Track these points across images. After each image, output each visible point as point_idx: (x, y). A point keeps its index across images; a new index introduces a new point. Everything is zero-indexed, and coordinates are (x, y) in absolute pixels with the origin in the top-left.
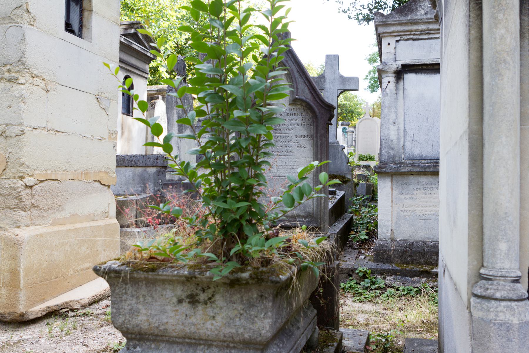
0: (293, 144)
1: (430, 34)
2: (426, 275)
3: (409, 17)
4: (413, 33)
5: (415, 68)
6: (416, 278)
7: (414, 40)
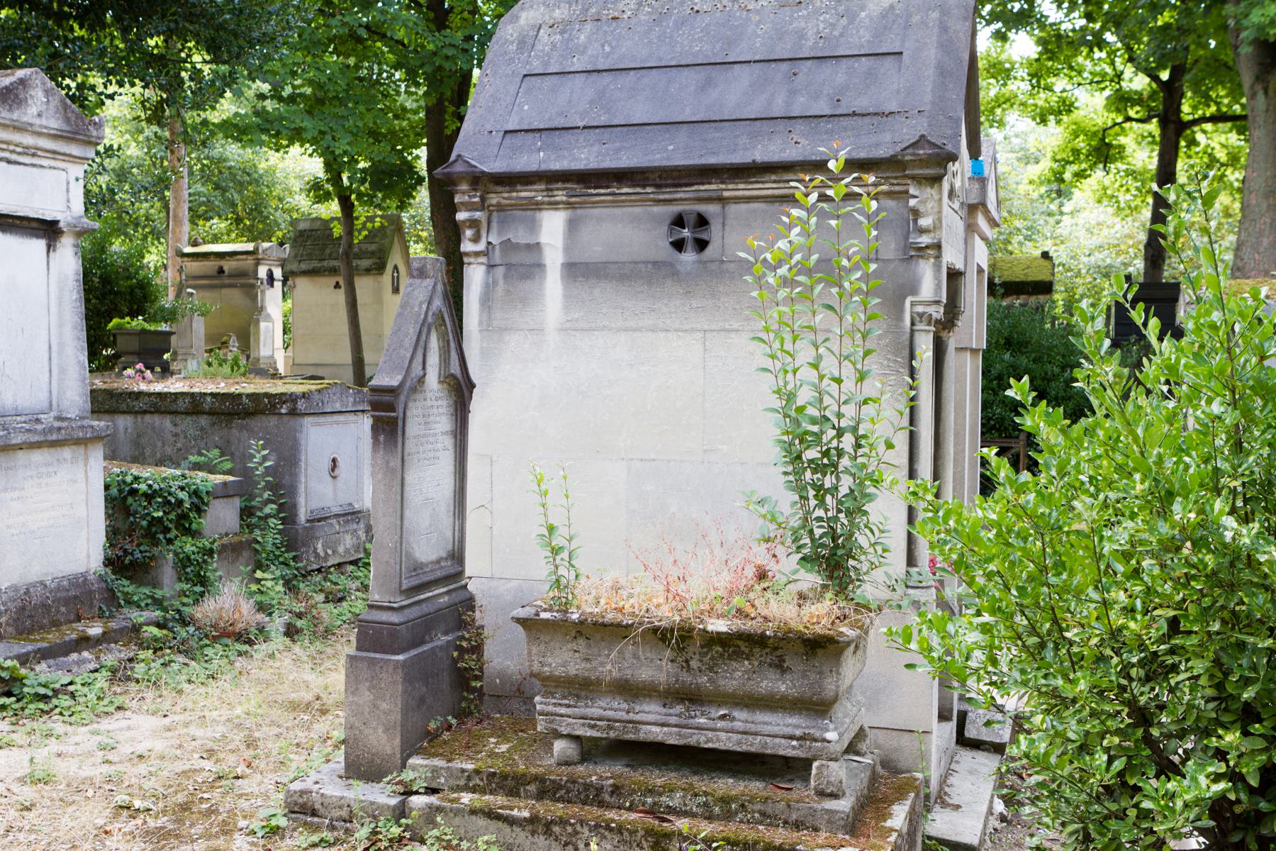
0: (439, 446)
1: (34, 155)
2: (84, 644)
3: (15, 116)
4: (12, 148)
5: (3, 220)
6: (74, 656)
7: (9, 162)
